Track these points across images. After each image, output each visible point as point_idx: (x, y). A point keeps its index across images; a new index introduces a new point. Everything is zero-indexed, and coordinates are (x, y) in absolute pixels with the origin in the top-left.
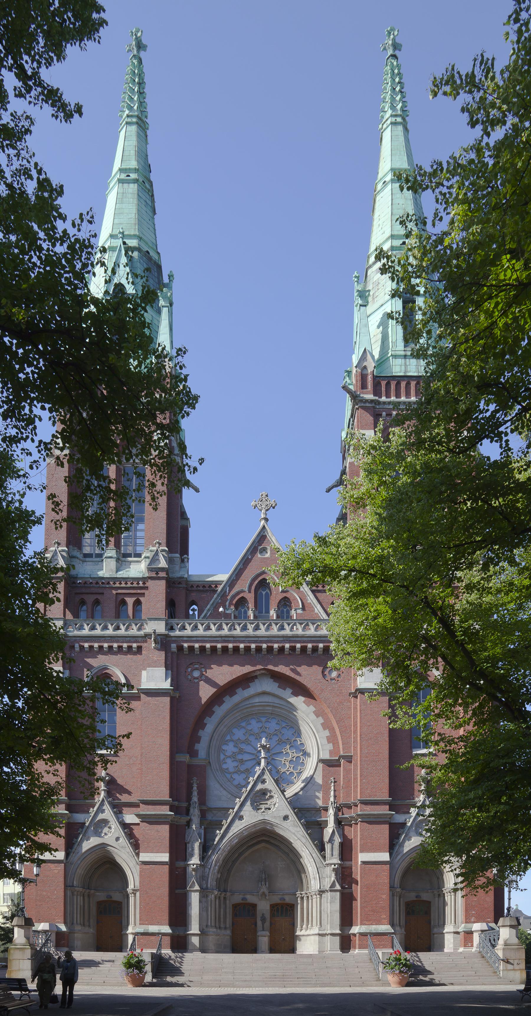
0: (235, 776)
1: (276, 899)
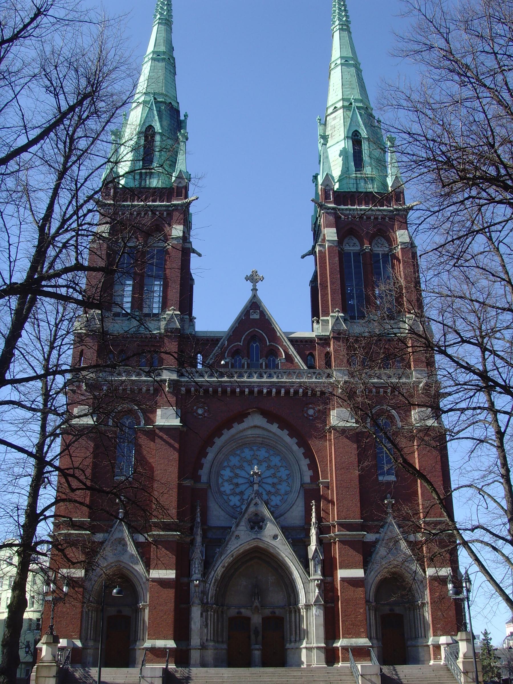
0: (231, 498)
1: (267, 612)
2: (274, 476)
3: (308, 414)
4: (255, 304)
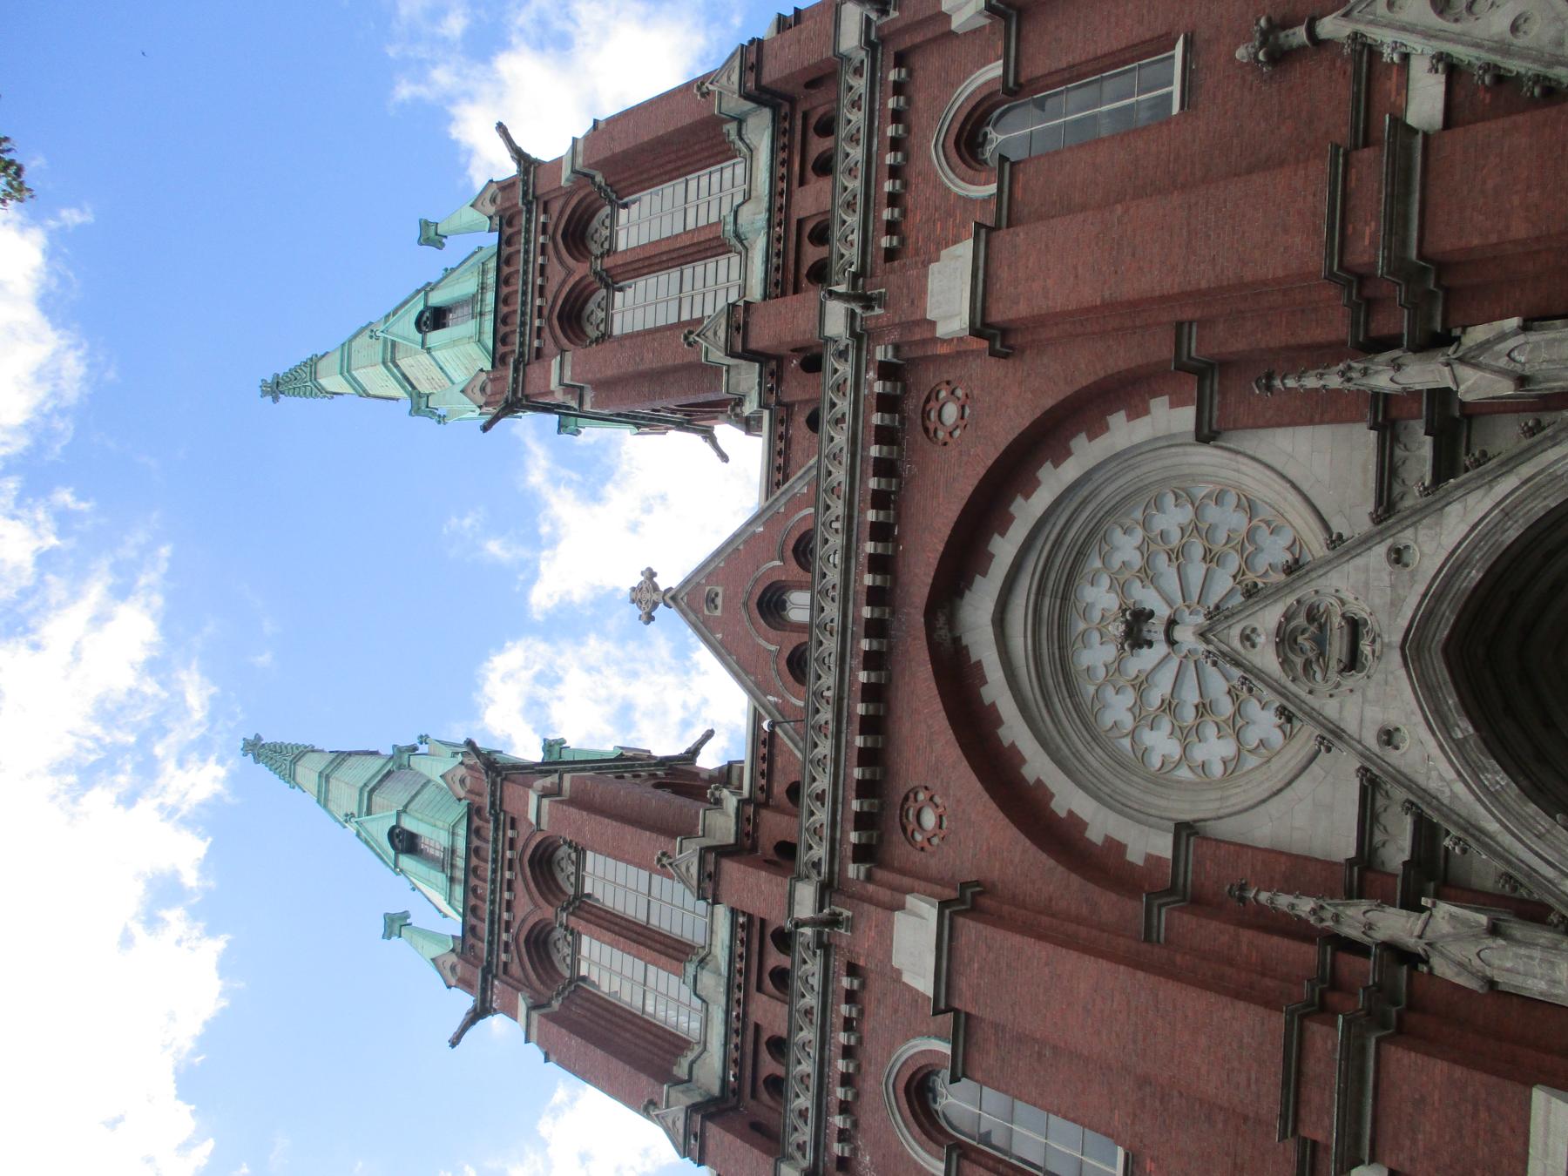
2: (1178, 555)
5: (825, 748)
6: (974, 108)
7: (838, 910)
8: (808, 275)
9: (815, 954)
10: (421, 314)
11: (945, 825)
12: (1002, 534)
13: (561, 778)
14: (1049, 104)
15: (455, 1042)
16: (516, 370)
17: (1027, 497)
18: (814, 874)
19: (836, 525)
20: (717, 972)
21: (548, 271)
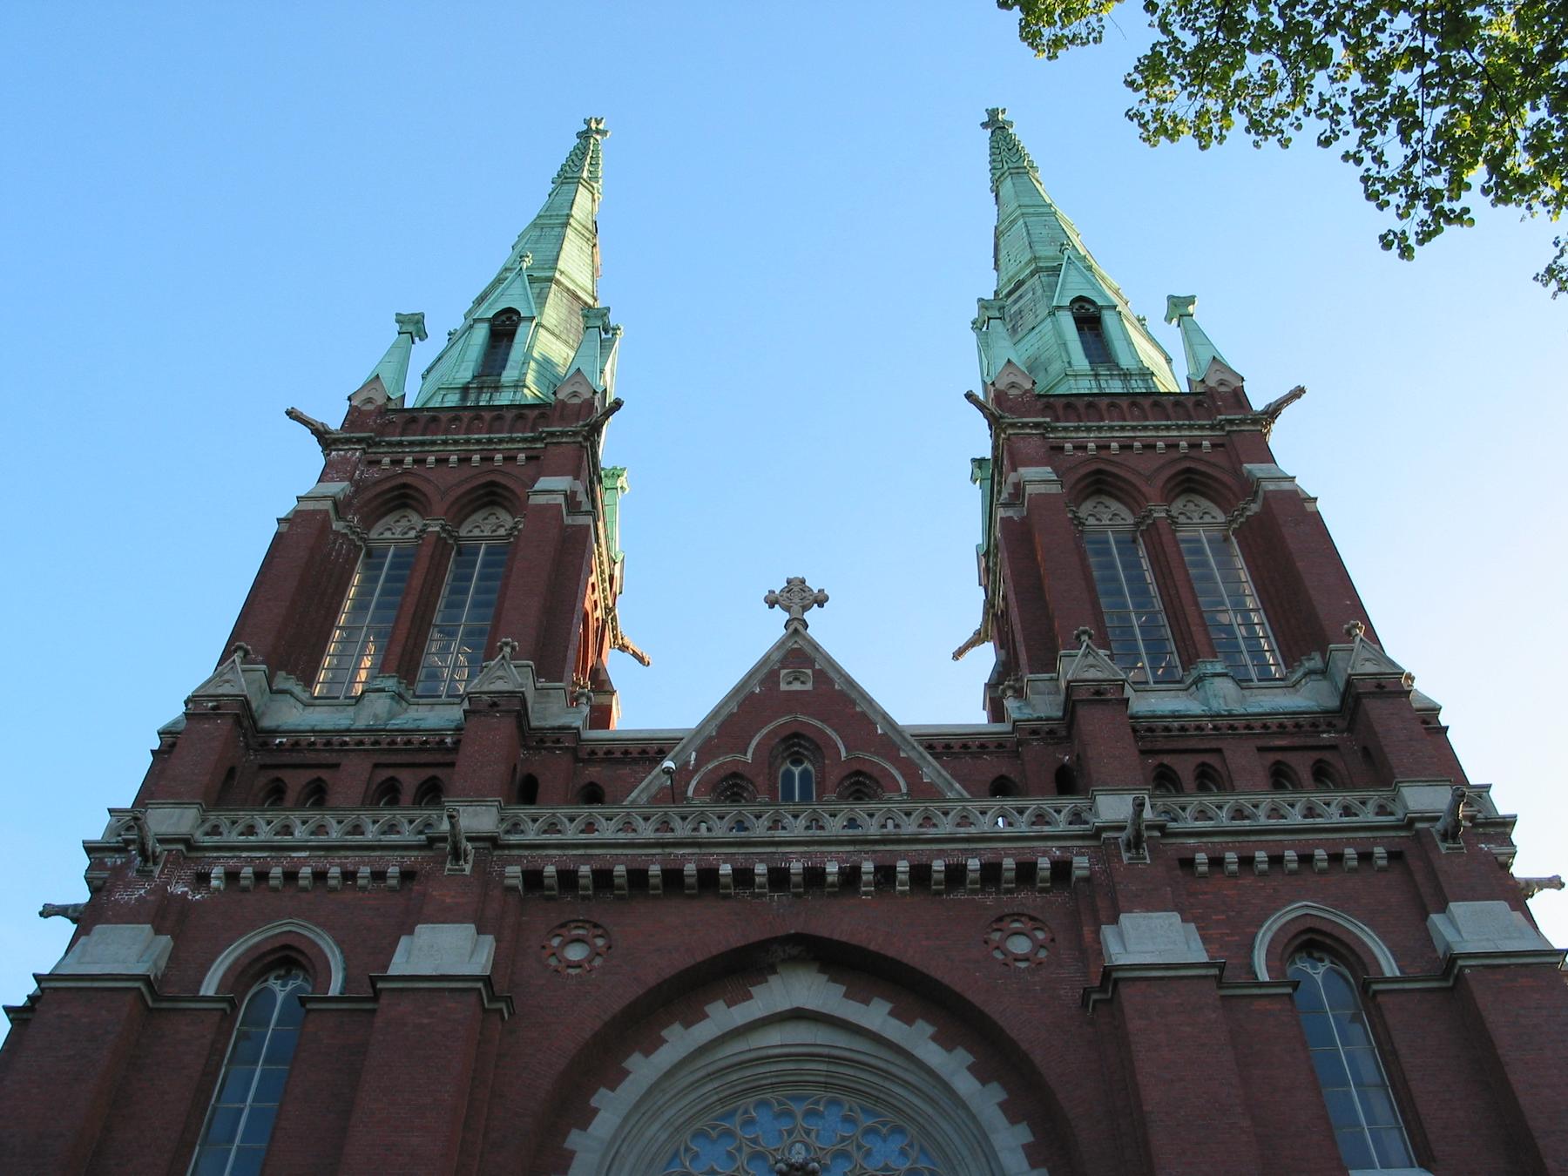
3: (1006, 953)
4: (798, 653)
5: (647, 832)
6: (1348, 946)
7: (471, 858)
8: (1161, 765)
9: (421, 833)
10: (1093, 303)
11: (571, 971)
12: (892, 1013)
13: (587, 513)
14: (1357, 1028)
15: (292, 414)
16: (1037, 425)
17: (934, 1038)
18: (504, 826)
19: (890, 823)
20: (392, 715)
21: (1149, 453)
